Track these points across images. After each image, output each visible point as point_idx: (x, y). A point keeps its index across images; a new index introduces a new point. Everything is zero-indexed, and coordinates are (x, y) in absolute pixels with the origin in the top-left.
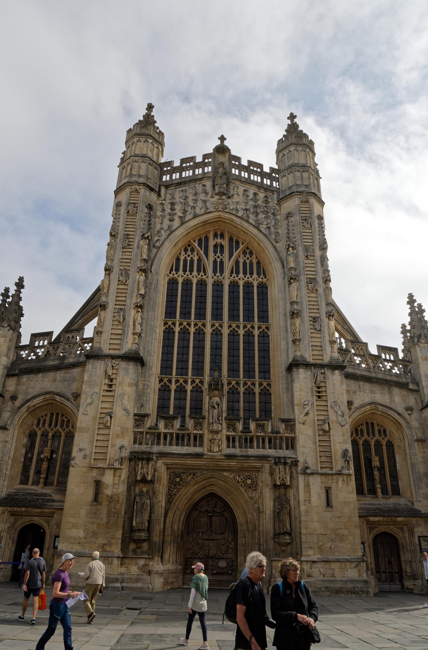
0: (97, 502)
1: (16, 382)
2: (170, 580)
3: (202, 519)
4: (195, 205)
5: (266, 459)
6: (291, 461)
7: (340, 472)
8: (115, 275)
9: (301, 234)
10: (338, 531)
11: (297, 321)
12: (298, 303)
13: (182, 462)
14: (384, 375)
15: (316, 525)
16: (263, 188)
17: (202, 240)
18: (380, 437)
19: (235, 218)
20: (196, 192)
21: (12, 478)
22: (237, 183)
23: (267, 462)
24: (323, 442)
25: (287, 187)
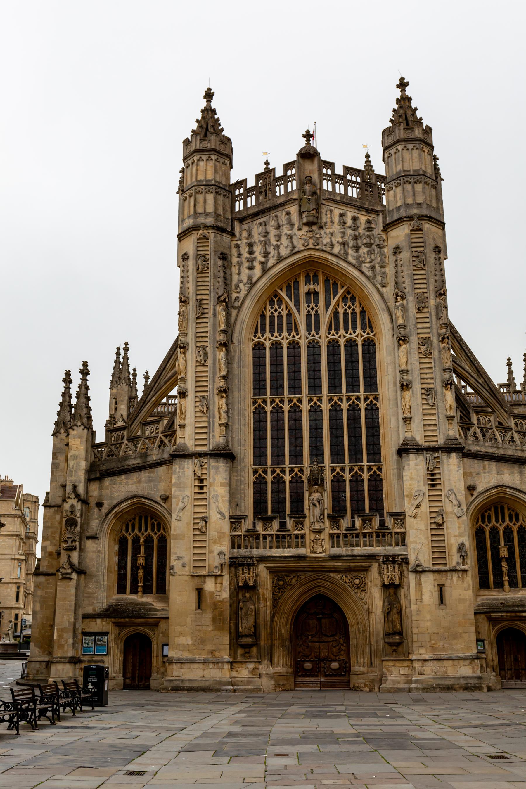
0: (202, 610)
1: (98, 486)
2: (281, 683)
3: (311, 622)
4: (279, 243)
5: (374, 557)
6: (402, 559)
7: (454, 568)
9: (412, 277)
10: (452, 629)
11: (407, 394)
12: (408, 371)
13: (284, 565)
14: (514, 451)
15: (429, 624)
16: (364, 208)
17: (291, 286)
18: (511, 523)
19: (329, 257)
20: (278, 224)
21: (109, 588)
22: (330, 204)
24: (437, 536)
25: (395, 206)
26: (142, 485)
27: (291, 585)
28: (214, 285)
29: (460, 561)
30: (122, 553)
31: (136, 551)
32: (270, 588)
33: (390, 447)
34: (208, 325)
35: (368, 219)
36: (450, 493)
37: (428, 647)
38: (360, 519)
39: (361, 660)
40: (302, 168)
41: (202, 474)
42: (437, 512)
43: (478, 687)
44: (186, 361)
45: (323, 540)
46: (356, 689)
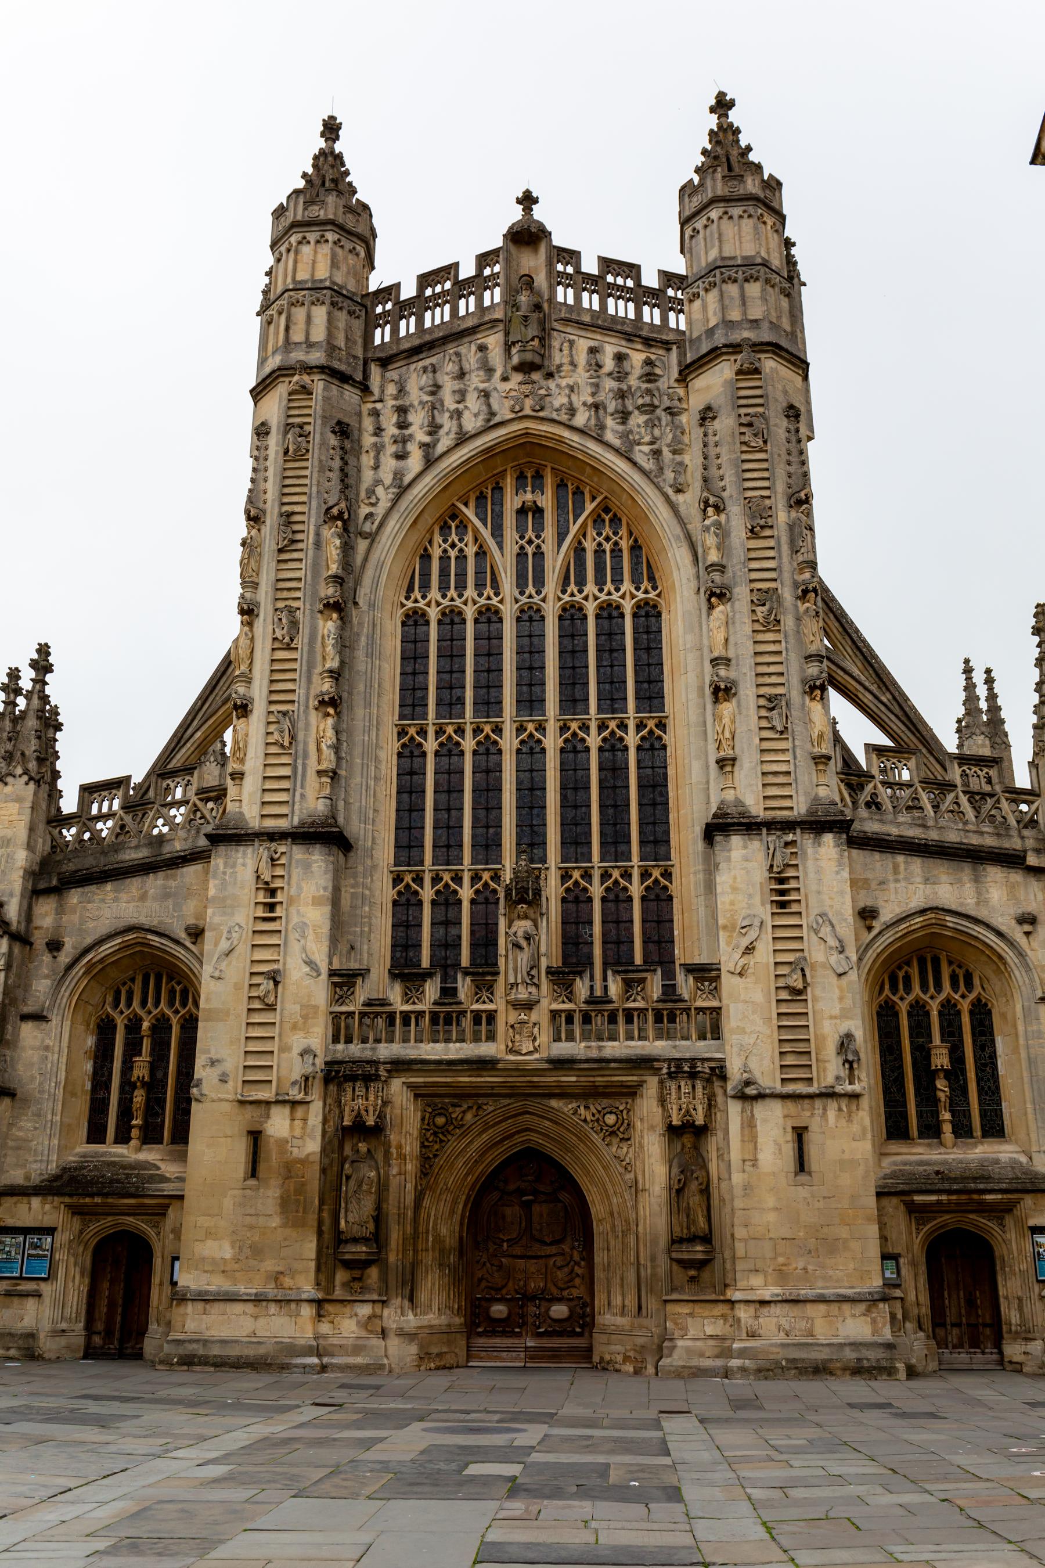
1: (54, 906)
2: (435, 1350)
3: (508, 1211)
4: (461, 406)
6: (712, 1069)
7: (830, 1090)
8: (264, 625)
9: (738, 467)
10: (825, 1230)
11: (727, 709)
12: (729, 660)
13: (448, 1080)
14: (962, 833)
19: (566, 434)
21: (66, 1129)
22: (569, 330)
23: (651, 1072)
24: (791, 1017)
25: (703, 329)
26: (148, 904)
27: (463, 1125)
28: (318, 484)
29: (844, 1073)
30: (102, 1054)
31: (133, 1048)
32: (416, 1133)
33: (690, 825)
34: (303, 566)
35: (648, 358)
36: (820, 921)
37: (770, 1271)
38: (619, 978)
39: (618, 1300)
40: (514, 263)
41: (273, 877)
42: (790, 963)
43: (885, 1368)
44: (252, 639)
45: (535, 1024)
46: (604, 1367)
